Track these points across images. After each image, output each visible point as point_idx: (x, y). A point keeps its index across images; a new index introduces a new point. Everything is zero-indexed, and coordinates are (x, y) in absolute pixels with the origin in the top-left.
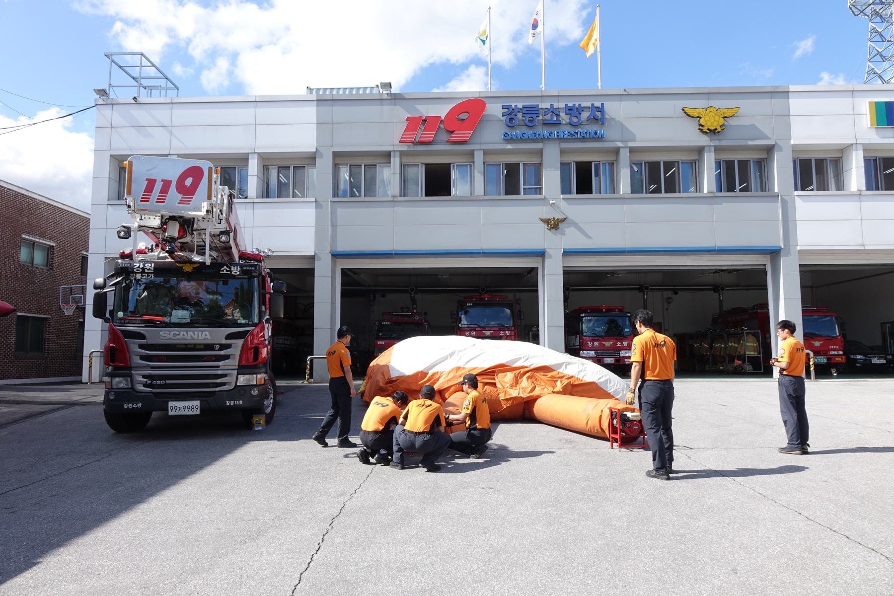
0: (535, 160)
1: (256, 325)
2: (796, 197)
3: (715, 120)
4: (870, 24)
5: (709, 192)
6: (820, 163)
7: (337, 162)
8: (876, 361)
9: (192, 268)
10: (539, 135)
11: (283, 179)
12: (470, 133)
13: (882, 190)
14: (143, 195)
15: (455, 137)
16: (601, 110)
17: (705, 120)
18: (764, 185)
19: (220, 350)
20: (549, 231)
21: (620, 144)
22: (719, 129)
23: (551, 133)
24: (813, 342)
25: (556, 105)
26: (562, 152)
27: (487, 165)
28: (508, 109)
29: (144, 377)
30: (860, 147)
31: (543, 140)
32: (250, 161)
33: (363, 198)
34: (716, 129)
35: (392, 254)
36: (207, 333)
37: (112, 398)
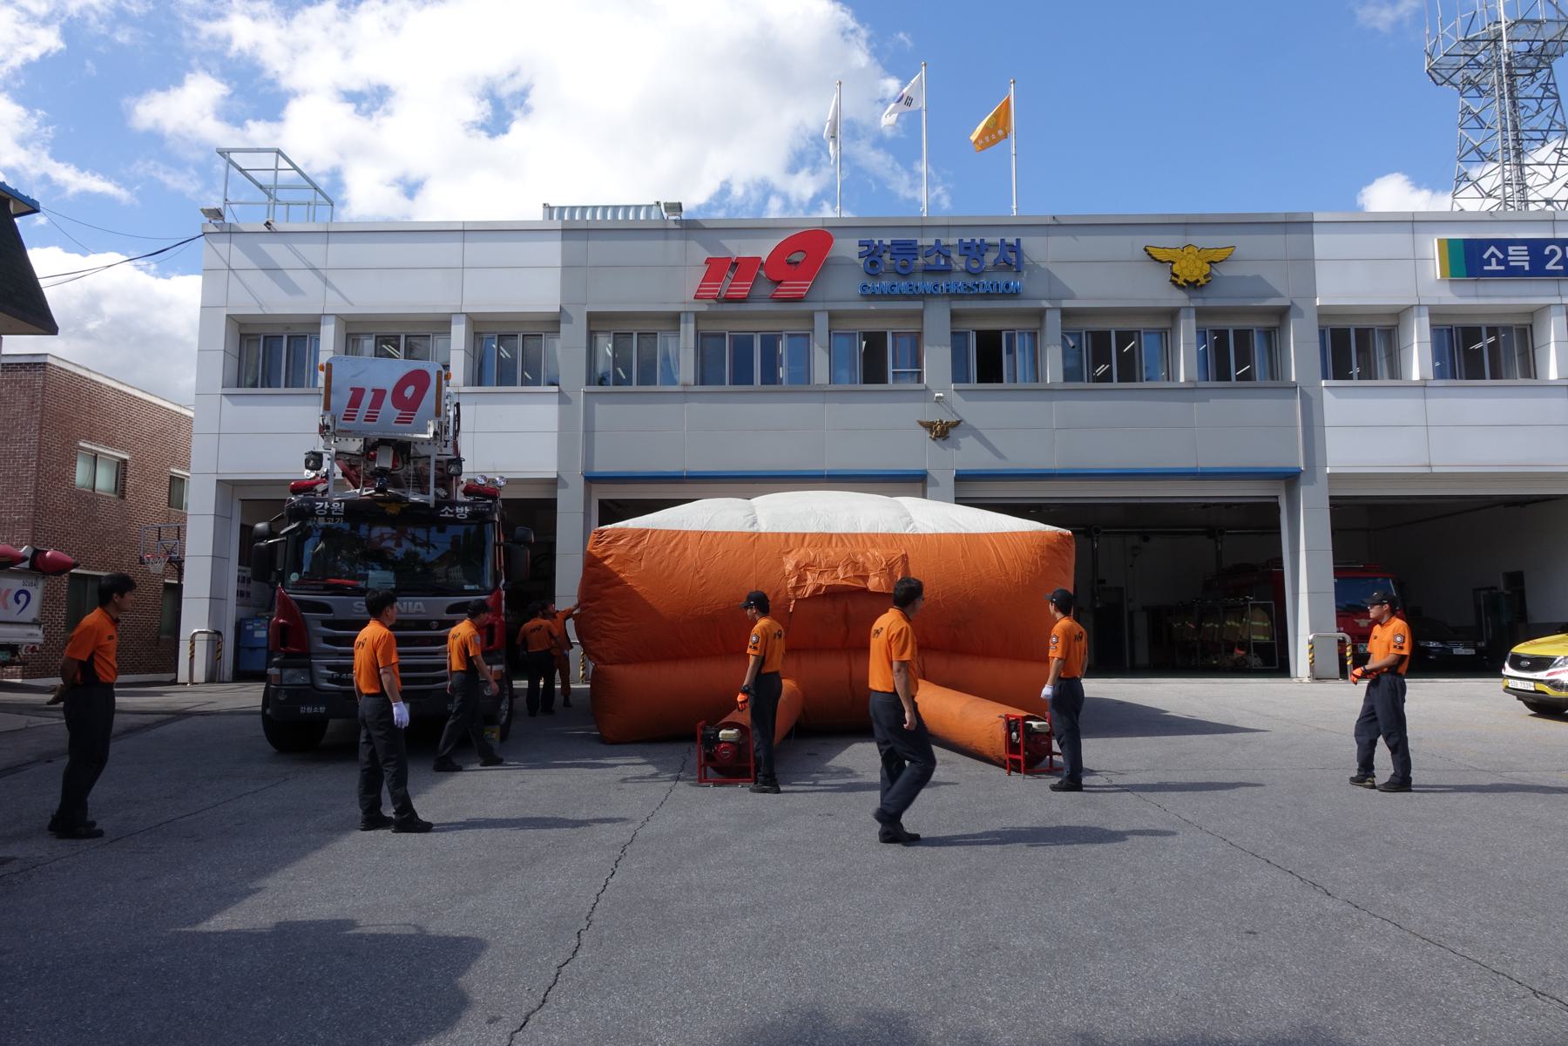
0: (911, 327)
1: (490, 593)
2: (1324, 390)
3: (1196, 267)
4: (1461, 99)
5: (1187, 380)
6: (1364, 335)
7: (592, 329)
8: (1460, 651)
9: (399, 510)
10: (917, 288)
11: (505, 354)
12: (807, 285)
13: (1461, 378)
14: (347, 411)
15: (786, 290)
16: (1016, 248)
17: (1180, 266)
18: (1275, 369)
19: (439, 629)
20: (933, 442)
21: (1045, 304)
22: (1203, 281)
23: (937, 285)
24: (1357, 621)
25: (944, 241)
26: (955, 316)
27: (835, 334)
28: (868, 246)
29: (329, 667)
30: (1425, 311)
31: (923, 296)
32: (453, 328)
33: (634, 388)
34: (1198, 281)
35: (682, 477)
36: (421, 604)
37: (282, 699)
